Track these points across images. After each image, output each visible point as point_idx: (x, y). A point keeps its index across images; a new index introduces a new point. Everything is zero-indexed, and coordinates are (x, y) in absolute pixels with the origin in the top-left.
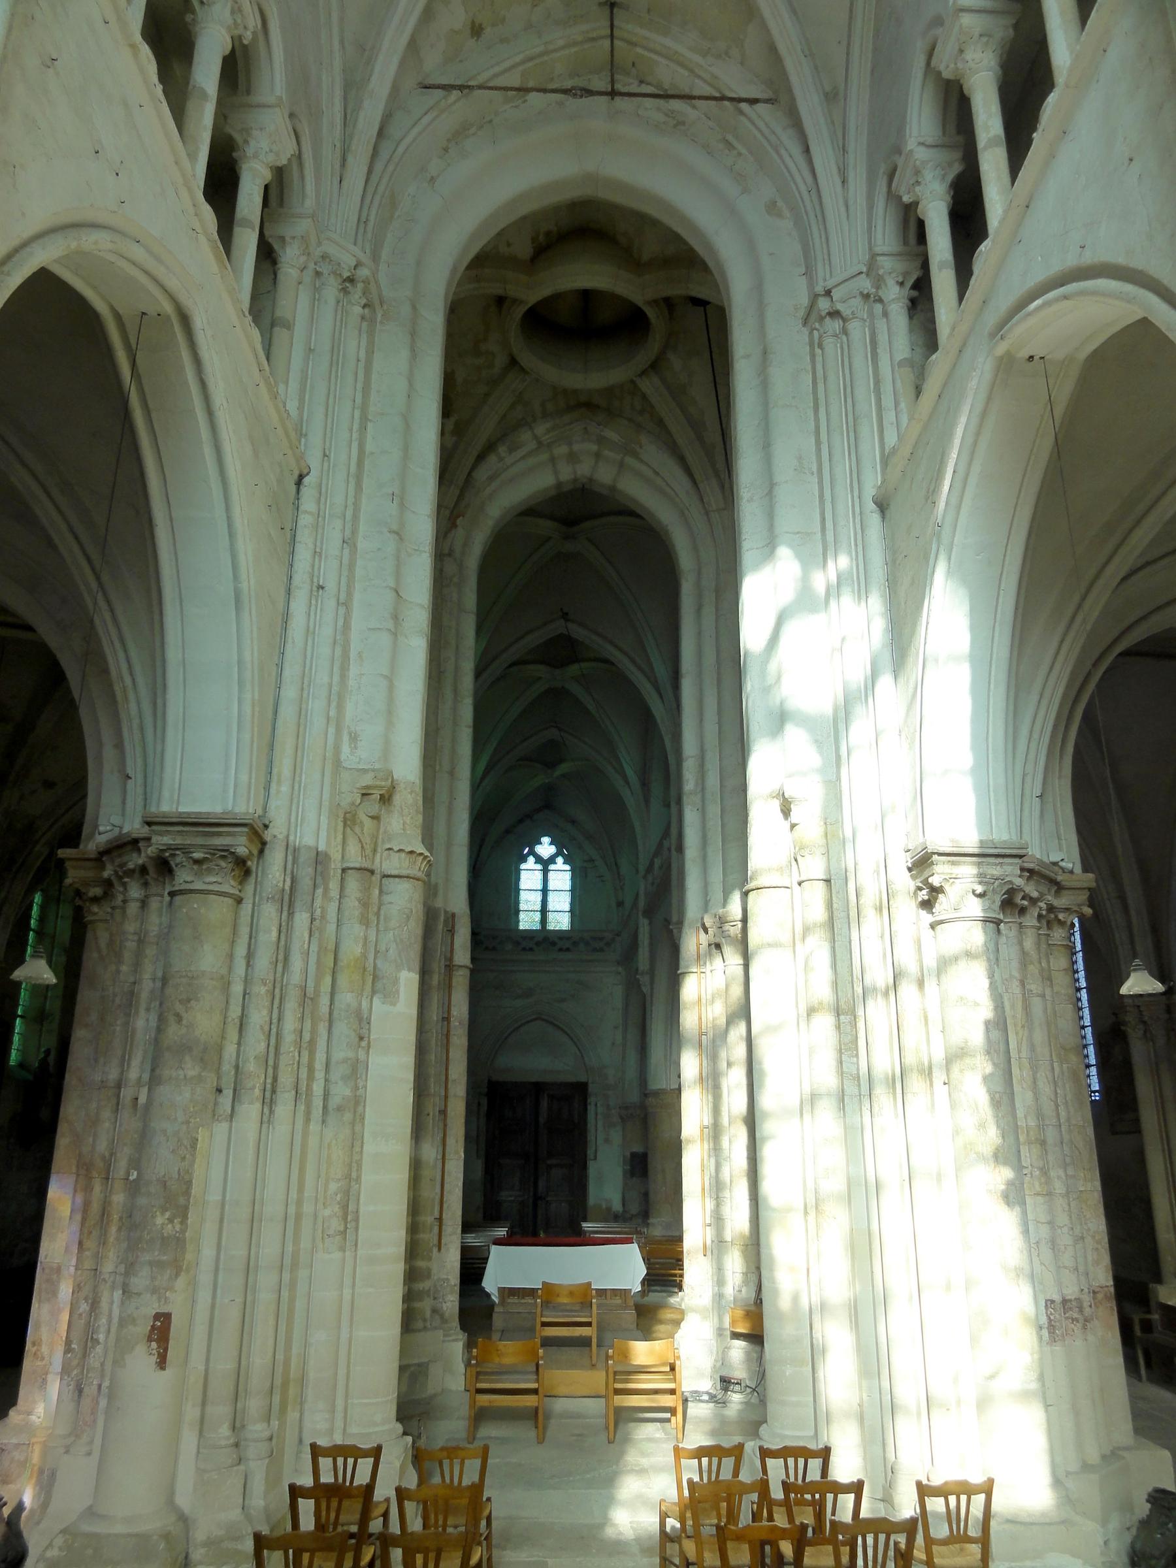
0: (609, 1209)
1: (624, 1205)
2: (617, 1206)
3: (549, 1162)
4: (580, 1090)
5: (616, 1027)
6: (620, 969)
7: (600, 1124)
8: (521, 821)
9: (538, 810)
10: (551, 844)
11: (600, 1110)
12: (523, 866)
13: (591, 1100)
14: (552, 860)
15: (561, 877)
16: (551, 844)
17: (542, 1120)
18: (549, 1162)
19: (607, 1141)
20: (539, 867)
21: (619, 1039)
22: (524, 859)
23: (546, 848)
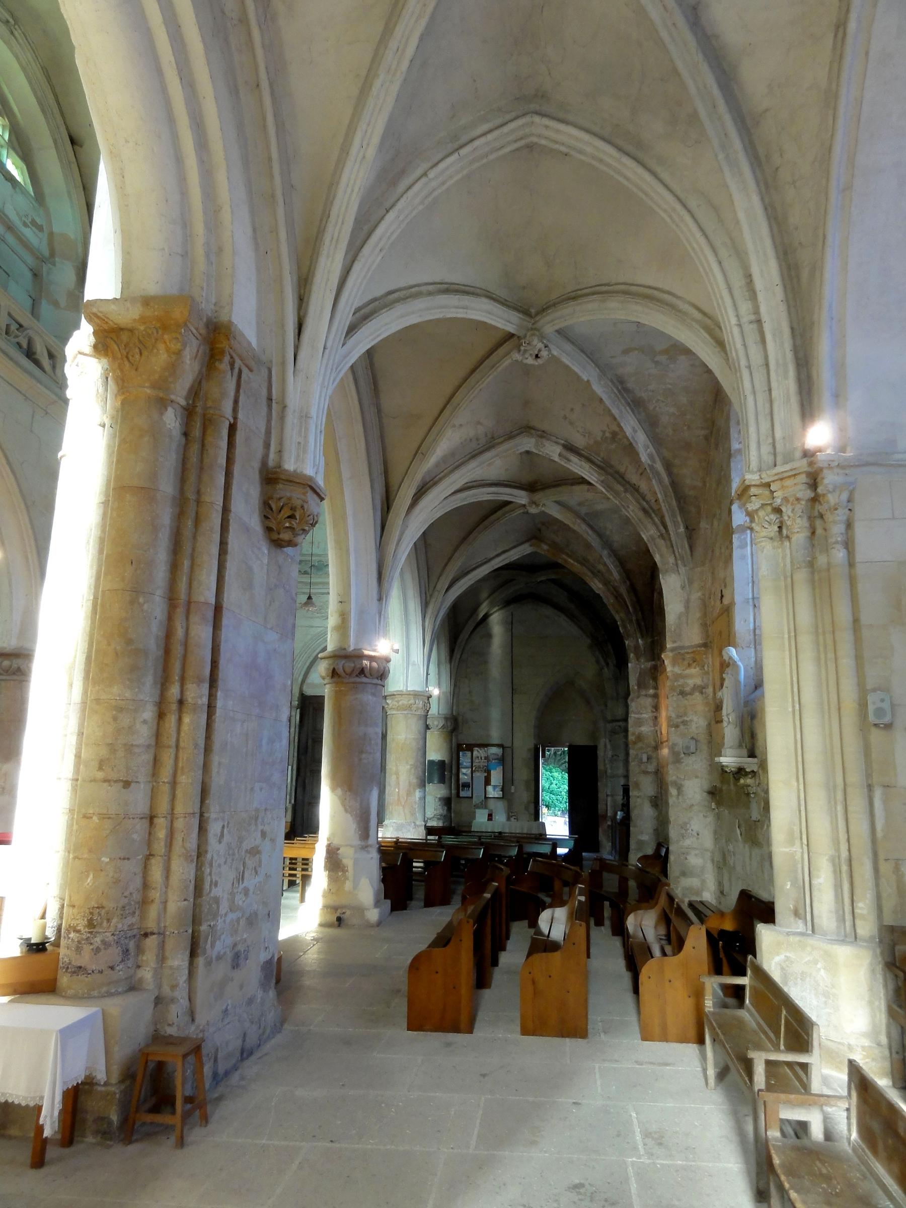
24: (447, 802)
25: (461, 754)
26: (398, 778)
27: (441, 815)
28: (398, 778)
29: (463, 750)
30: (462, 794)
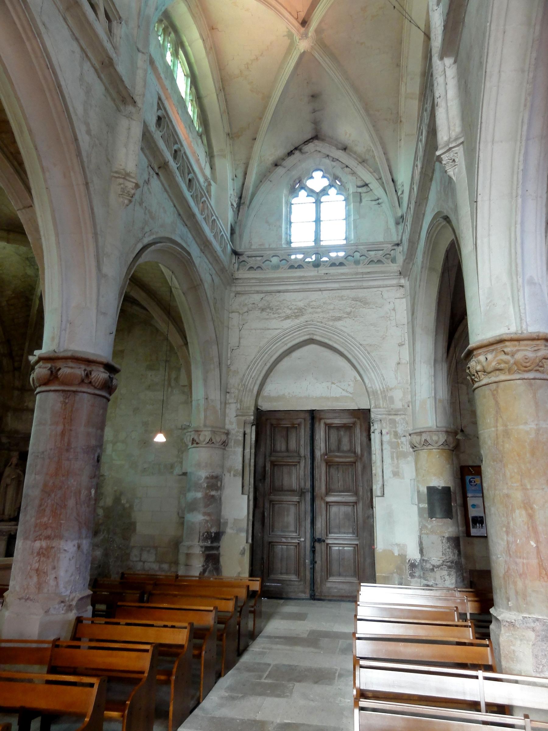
0: (402, 557)
1: (421, 551)
2: (413, 554)
3: (330, 499)
4: (363, 417)
5: (401, 345)
6: (403, 281)
7: (387, 454)
8: (290, 153)
9: (307, 142)
10: (323, 177)
11: (386, 438)
12: (294, 201)
13: (375, 427)
14: (324, 191)
15: (335, 205)
16: (323, 177)
17: (318, 454)
18: (330, 499)
19: (396, 474)
20: (313, 200)
21: (406, 356)
22: (293, 192)
23: (317, 181)
24: (455, 542)
25: (468, 478)
26: (531, 517)
27: (452, 562)
28: (531, 517)
29: (471, 474)
30: (474, 532)
